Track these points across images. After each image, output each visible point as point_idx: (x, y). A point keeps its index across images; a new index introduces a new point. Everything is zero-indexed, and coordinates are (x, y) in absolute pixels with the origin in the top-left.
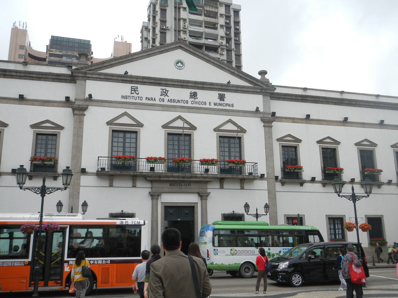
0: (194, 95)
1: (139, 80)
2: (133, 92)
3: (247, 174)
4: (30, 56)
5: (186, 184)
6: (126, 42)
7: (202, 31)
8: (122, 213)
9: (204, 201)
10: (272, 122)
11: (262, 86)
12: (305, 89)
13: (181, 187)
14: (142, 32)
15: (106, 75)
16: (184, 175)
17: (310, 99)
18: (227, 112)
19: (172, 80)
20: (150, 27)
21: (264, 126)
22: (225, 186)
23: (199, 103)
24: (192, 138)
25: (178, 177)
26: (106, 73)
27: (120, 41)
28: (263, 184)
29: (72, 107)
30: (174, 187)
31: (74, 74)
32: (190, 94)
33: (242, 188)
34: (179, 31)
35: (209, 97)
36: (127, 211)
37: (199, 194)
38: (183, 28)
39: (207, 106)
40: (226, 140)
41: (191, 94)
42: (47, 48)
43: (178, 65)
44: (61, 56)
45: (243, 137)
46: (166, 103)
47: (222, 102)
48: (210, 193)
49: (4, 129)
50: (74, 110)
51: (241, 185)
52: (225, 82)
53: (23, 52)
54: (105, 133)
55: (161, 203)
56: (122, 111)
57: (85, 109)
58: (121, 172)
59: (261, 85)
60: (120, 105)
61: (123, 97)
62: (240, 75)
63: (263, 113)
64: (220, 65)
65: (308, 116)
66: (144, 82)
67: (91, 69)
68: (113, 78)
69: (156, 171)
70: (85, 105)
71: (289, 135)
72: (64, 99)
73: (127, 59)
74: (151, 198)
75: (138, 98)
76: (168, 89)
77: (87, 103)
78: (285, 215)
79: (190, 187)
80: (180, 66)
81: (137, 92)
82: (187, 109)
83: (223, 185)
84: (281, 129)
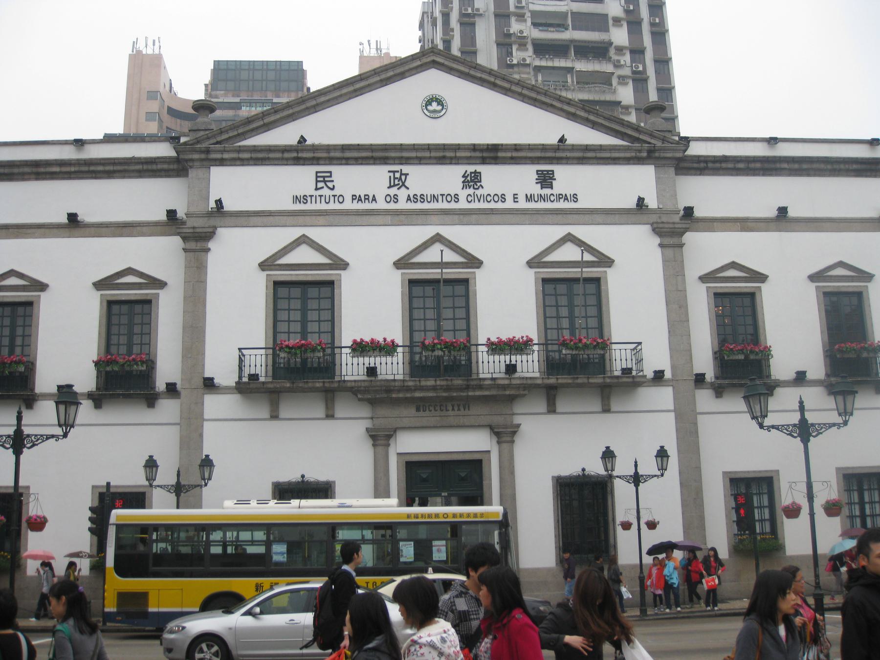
0: (472, 181)
1: (332, 154)
2: (320, 185)
3: (618, 373)
4: (172, 112)
5: (459, 406)
6: (387, 54)
7: (564, 9)
8: (303, 481)
9: (505, 445)
10: (682, 234)
11: (652, 141)
12: (772, 141)
13: (444, 413)
14: (421, 26)
15: (255, 149)
16: (449, 383)
17: (785, 166)
18: (560, 216)
19: (414, 147)
20: (437, 14)
21: (661, 245)
22: (562, 405)
23: (485, 198)
24: (471, 288)
25: (434, 388)
26: (255, 146)
27: (373, 53)
28: (664, 396)
29: (178, 234)
30: (427, 413)
31: (182, 156)
32: (463, 176)
33: (606, 410)
34: (507, 16)
35: (512, 182)
36: (316, 475)
37: (491, 428)
38: (517, 7)
39: (509, 204)
40: (562, 288)
41: (466, 177)
42: (206, 90)
43: (429, 108)
44: (236, 106)
45: (606, 278)
46: (402, 205)
47: (547, 191)
48: (518, 426)
49: (39, 296)
50: (185, 239)
51: (602, 401)
52: (553, 140)
53: (154, 106)
54: (258, 289)
55: (398, 454)
56: (295, 233)
57: (209, 235)
58: (293, 383)
59: (649, 140)
60: (290, 220)
61: (296, 199)
62: (592, 117)
63: (659, 211)
64: (539, 97)
65: (783, 211)
66: (347, 159)
67: (219, 139)
68: (272, 155)
69: (380, 377)
70: (209, 227)
71: (733, 265)
72: (163, 217)
73: (303, 107)
74: (372, 442)
75: (332, 198)
76: (406, 169)
77: (213, 222)
78: (725, 473)
79: (467, 412)
80: (435, 111)
81: (330, 185)
82: (456, 217)
83: (554, 404)
84: (707, 251)
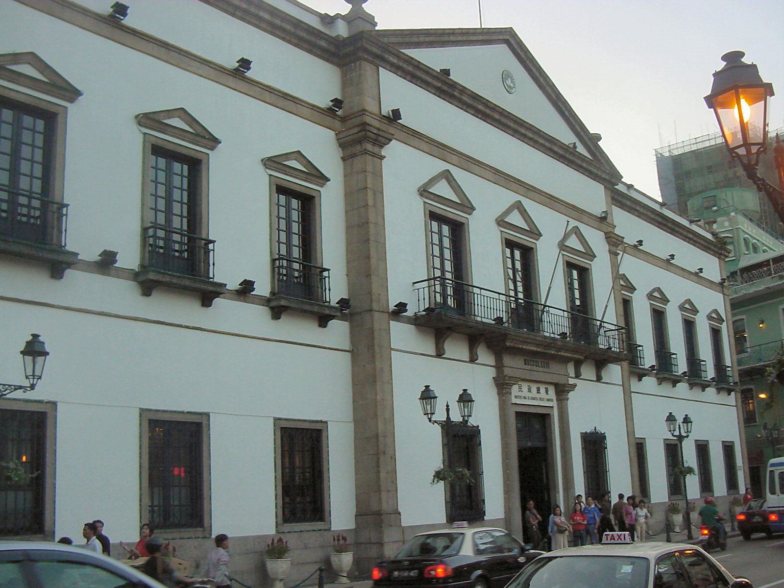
80: (509, 87)
